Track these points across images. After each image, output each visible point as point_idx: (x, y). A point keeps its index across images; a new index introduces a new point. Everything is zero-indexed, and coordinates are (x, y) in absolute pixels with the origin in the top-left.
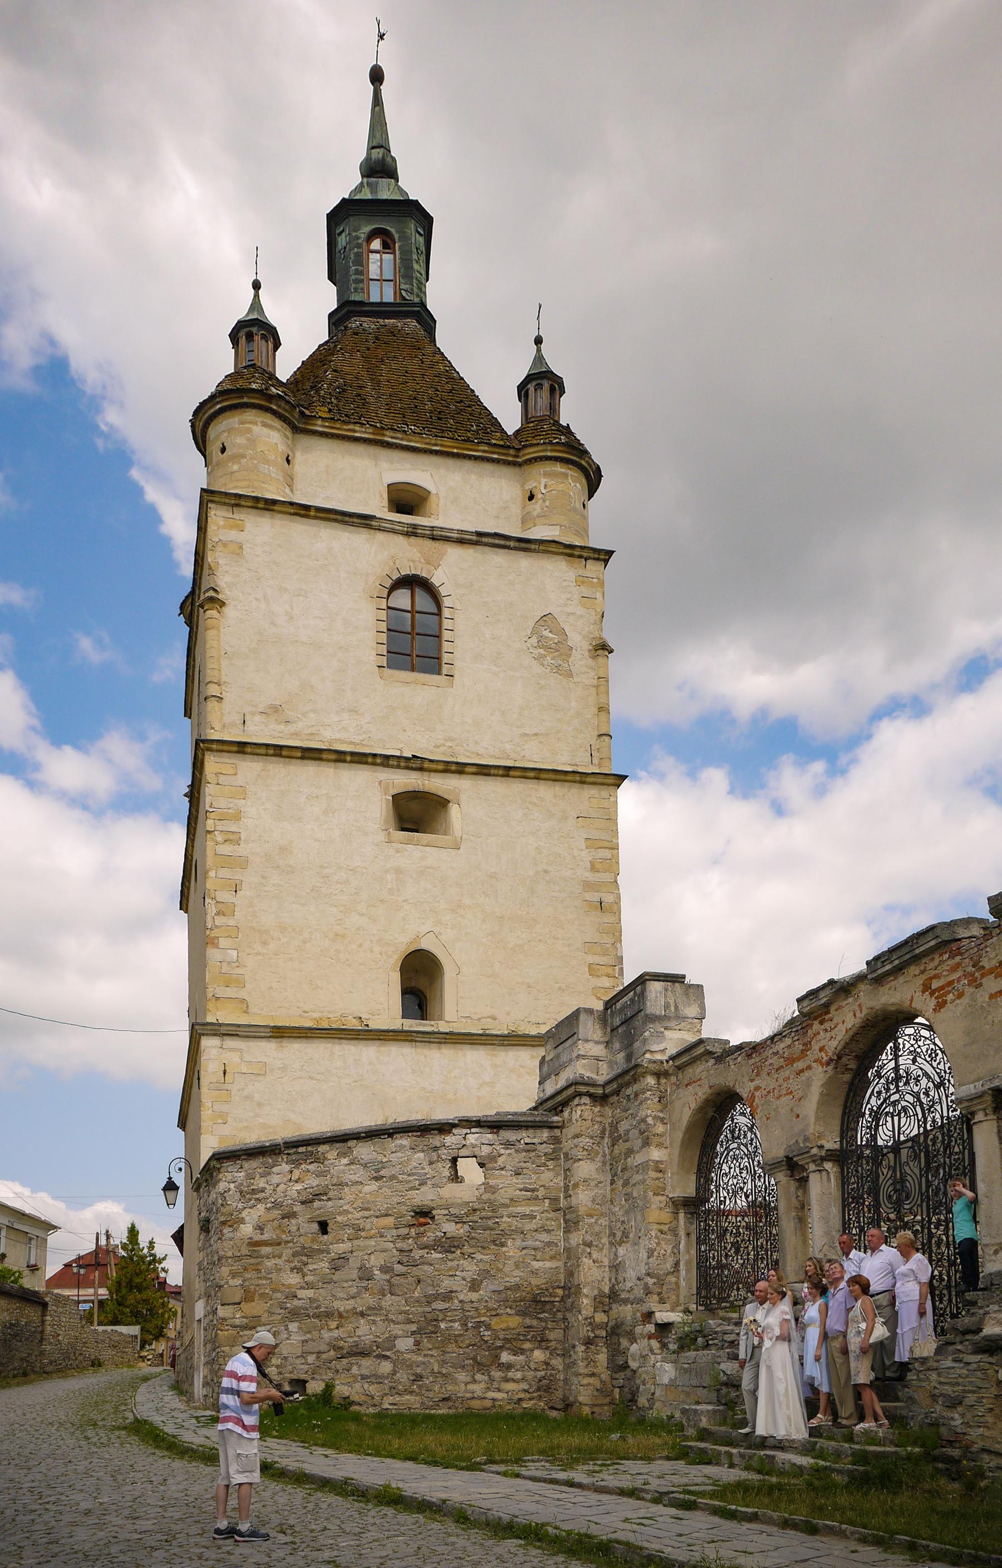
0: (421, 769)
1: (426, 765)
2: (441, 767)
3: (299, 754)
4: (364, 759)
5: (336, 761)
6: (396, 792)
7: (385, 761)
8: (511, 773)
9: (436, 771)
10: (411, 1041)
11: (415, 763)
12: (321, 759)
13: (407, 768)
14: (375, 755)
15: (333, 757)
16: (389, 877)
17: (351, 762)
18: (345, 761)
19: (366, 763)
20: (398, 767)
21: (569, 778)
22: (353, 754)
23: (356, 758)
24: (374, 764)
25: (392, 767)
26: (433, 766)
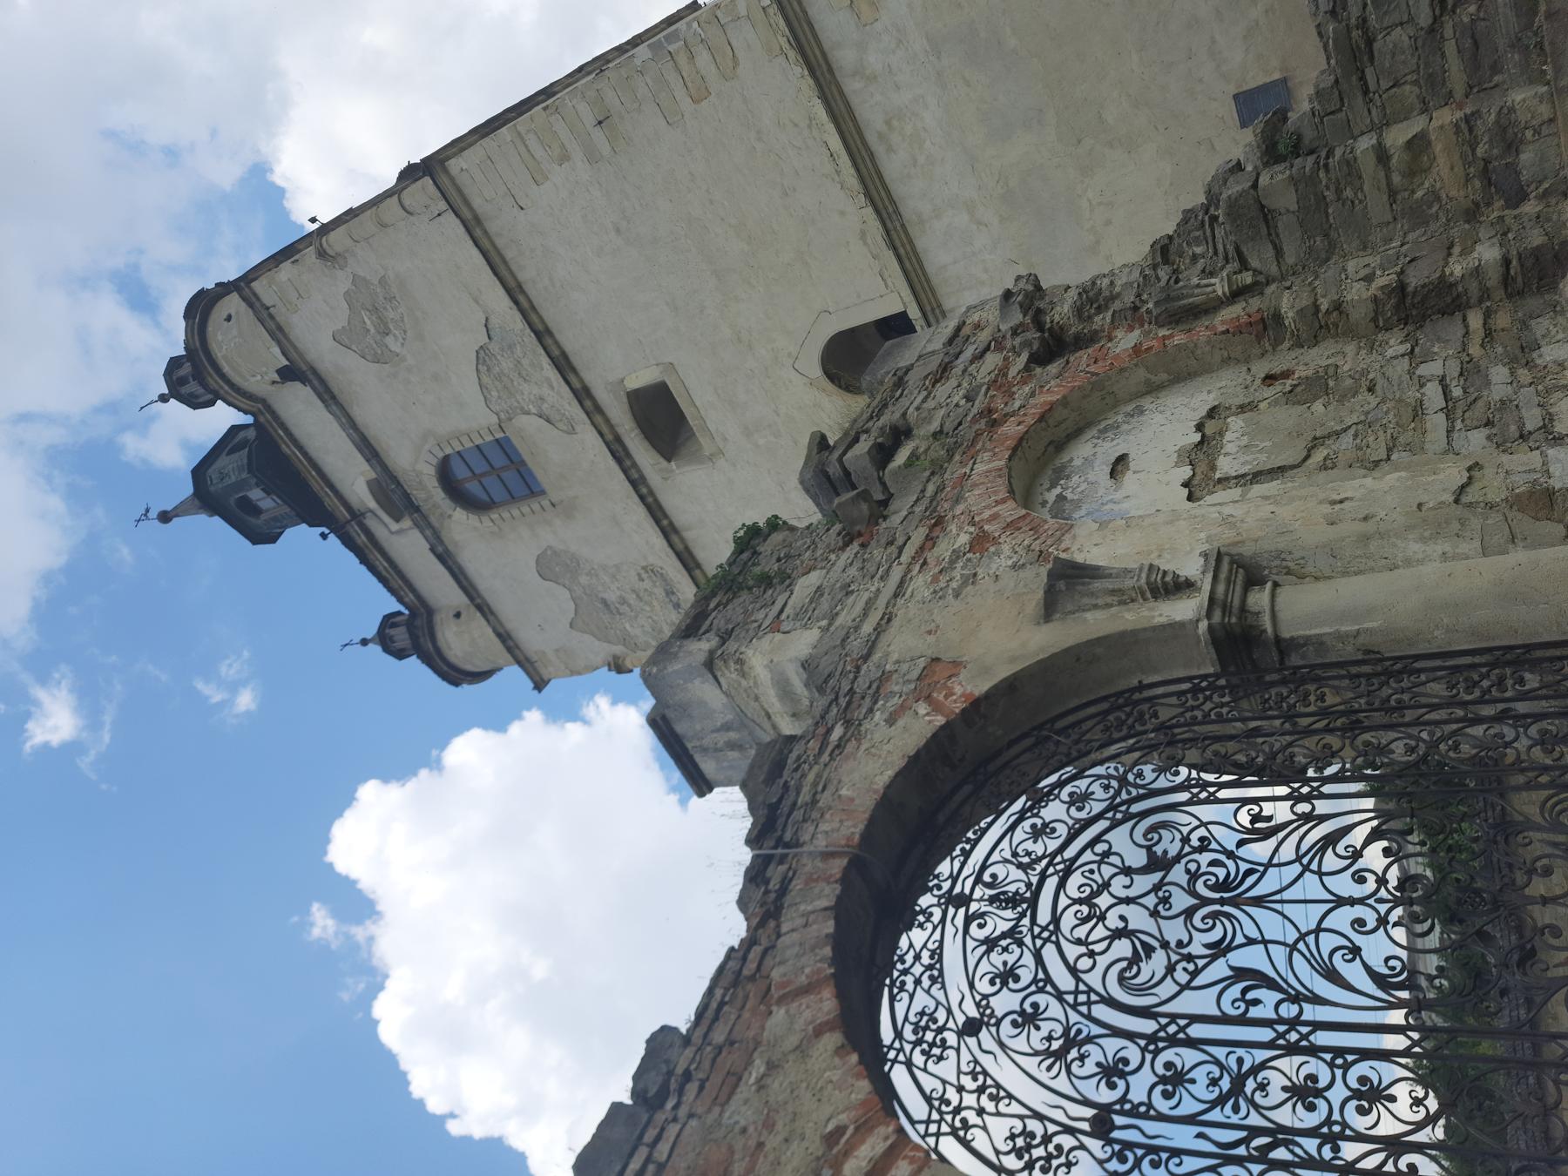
0: (618, 439)
1: (610, 437)
2: (598, 419)
3: (697, 572)
4: (654, 506)
5: (676, 531)
6: (664, 463)
7: (637, 482)
9: (607, 421)
11: (620, 454)
12: (687, 548)
13: (628, 455)
14: (642, 498)
15: (675, 539)
16: (761, 442)
17: (666, 516)
18: (671, 524)
20: (635, 465)
22: (657, 522)
23: (659, 514)
24: (651, 493)
25: (639, 471)
26: (605, 430)
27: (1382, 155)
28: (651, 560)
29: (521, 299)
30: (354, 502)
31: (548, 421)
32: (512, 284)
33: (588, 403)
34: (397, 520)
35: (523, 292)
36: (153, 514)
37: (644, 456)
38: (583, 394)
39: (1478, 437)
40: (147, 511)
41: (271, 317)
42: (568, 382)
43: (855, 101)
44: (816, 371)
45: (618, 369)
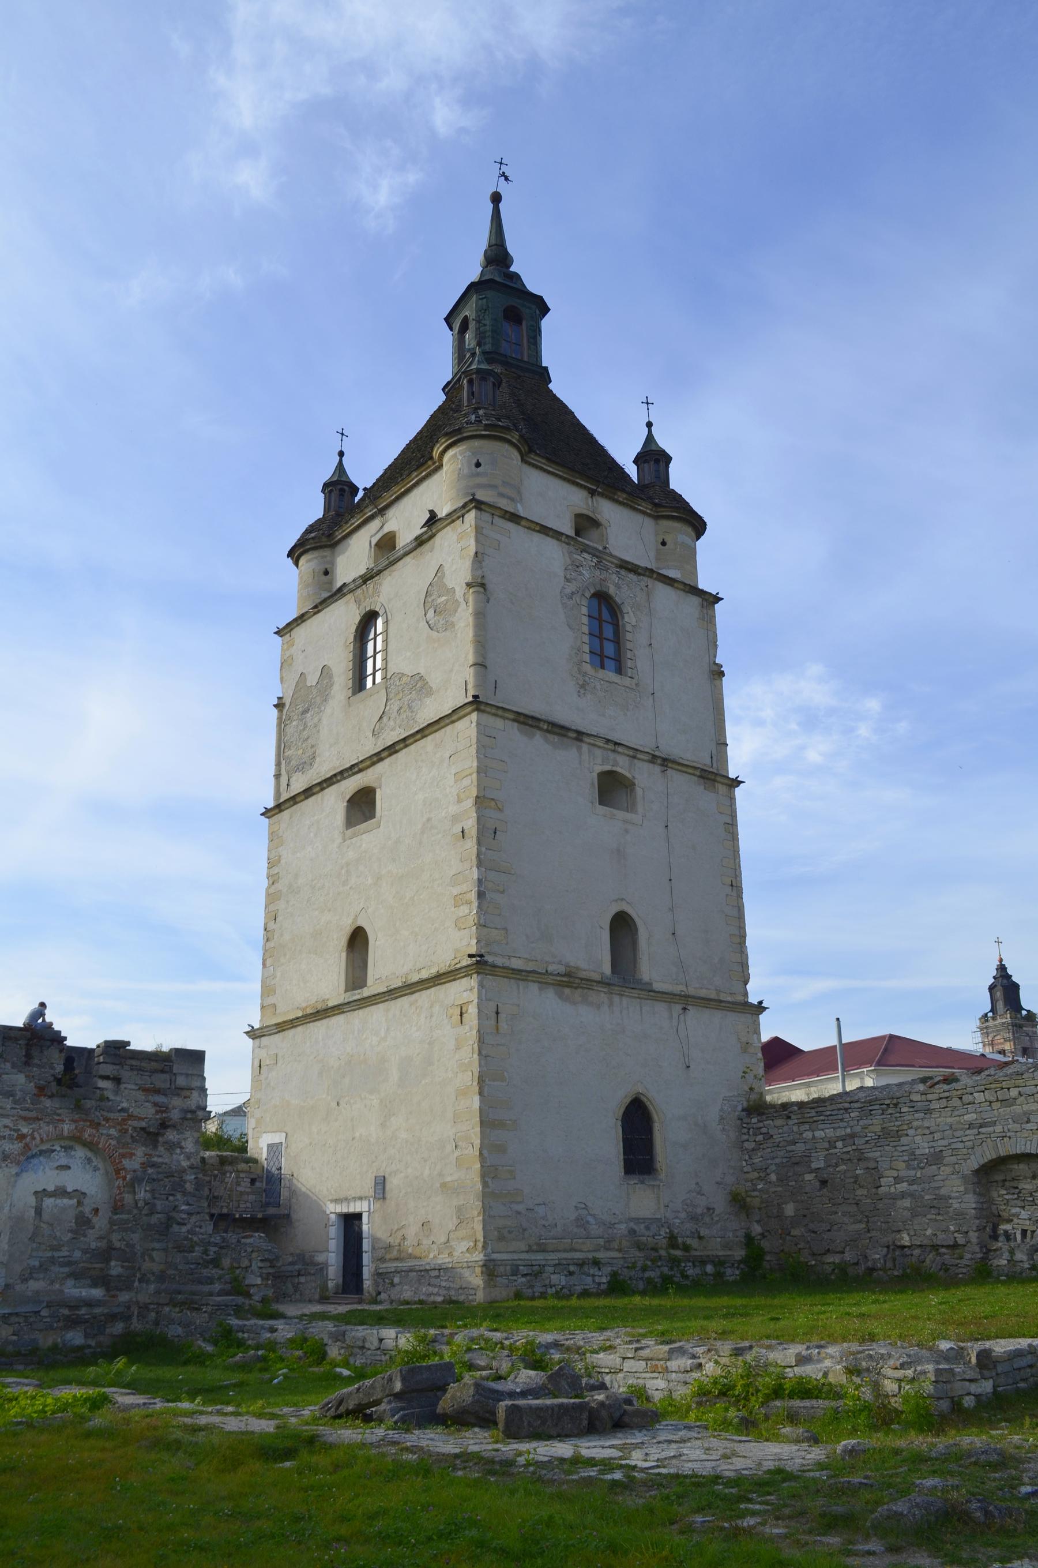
0: (360, 771)
2: (368, 763)
8: (408, 742)
10: (343, 1012)
13: (354, 774)
14: (335, 775)
17: (328, 786)
19: (334, 783)
20: (350, 776)
21: (442, 724)
24: (338, 781)
27: (153, 1249)
28: (318, 759)
29: (419, 736)
30: (391, 513)
31: (381, 717)
32: (427, 732)
33: (375, 759)
34: (376, 545)
35: (423, 737)
36: (503, 188)
37: (351, 785)
38: (377, 758)
39: (37, 1263)
40: (506, 179)
41: (458, 518)
42: (384, 750)
43: (428, 992)
44: (359, 924)
45: (390, 781)
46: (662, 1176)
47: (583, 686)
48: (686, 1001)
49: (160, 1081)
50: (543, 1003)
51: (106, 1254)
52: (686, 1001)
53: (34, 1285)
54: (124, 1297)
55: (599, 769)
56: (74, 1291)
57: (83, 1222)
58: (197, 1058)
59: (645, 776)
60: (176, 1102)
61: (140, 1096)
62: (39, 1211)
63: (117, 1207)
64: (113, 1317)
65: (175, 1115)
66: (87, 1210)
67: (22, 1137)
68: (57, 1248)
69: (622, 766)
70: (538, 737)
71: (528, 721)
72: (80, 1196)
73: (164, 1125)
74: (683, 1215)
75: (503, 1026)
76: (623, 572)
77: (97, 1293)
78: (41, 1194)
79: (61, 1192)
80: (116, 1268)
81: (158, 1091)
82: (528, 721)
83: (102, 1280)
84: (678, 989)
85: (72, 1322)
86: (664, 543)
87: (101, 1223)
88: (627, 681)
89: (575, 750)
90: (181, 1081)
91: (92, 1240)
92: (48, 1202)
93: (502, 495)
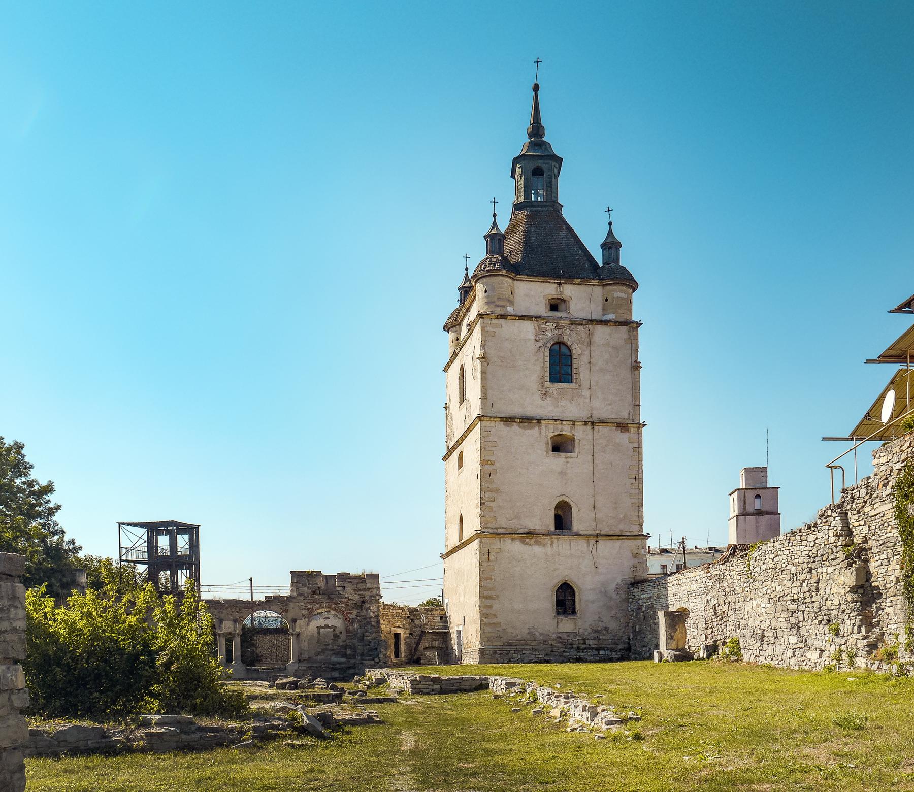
46: (578, 615)
47: (545, 394)
48: (597, 536)
49: (361, 586)
50: (515, 547)
51: (346, 647)
52: (597, 536)
53: (320, 657)
54: (353, 661)
55: (552, 434)
56: (335, 659)
57: (336, 637)
58: (376, 576)
59: (581, 433)
60: (367, 593)
61: (353, 592)
62: (319, 633)
63: (348, 631)
64: (349, 668)
65: (367, 598)
66: (337, 632)
67: (309, 609)
68: (328, 645)
69: (566, 430)
70: (515, 427)
71: (508, 420)
72: (334, 628)
73: (363, 602)
74: (590, 630)
75: (492, 558)
76: (573, 326)
77: (343, 660)
78: (319, 628)
79: (326, 627)
80: (349, 652)
81: (360, 590)
82: (508, 420)
83: (344, 655)
84: (595, 533)
85: (333, 669)
86: (607, 300)
87: (343, 636)
88: (573, 385)
89: (537, 428)
90: (369, 585)
91: (340, 642)
92: (322, 630)
93: (498, 306)
